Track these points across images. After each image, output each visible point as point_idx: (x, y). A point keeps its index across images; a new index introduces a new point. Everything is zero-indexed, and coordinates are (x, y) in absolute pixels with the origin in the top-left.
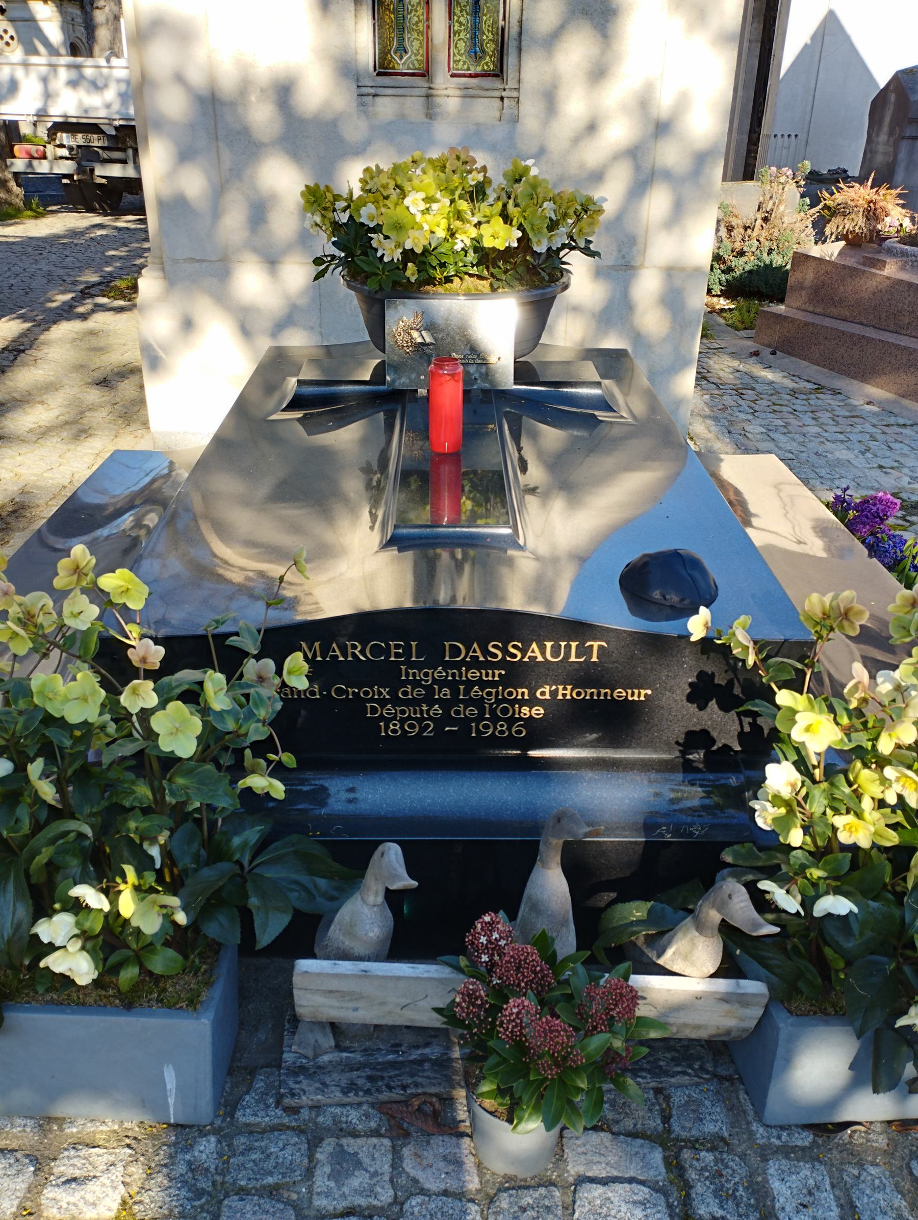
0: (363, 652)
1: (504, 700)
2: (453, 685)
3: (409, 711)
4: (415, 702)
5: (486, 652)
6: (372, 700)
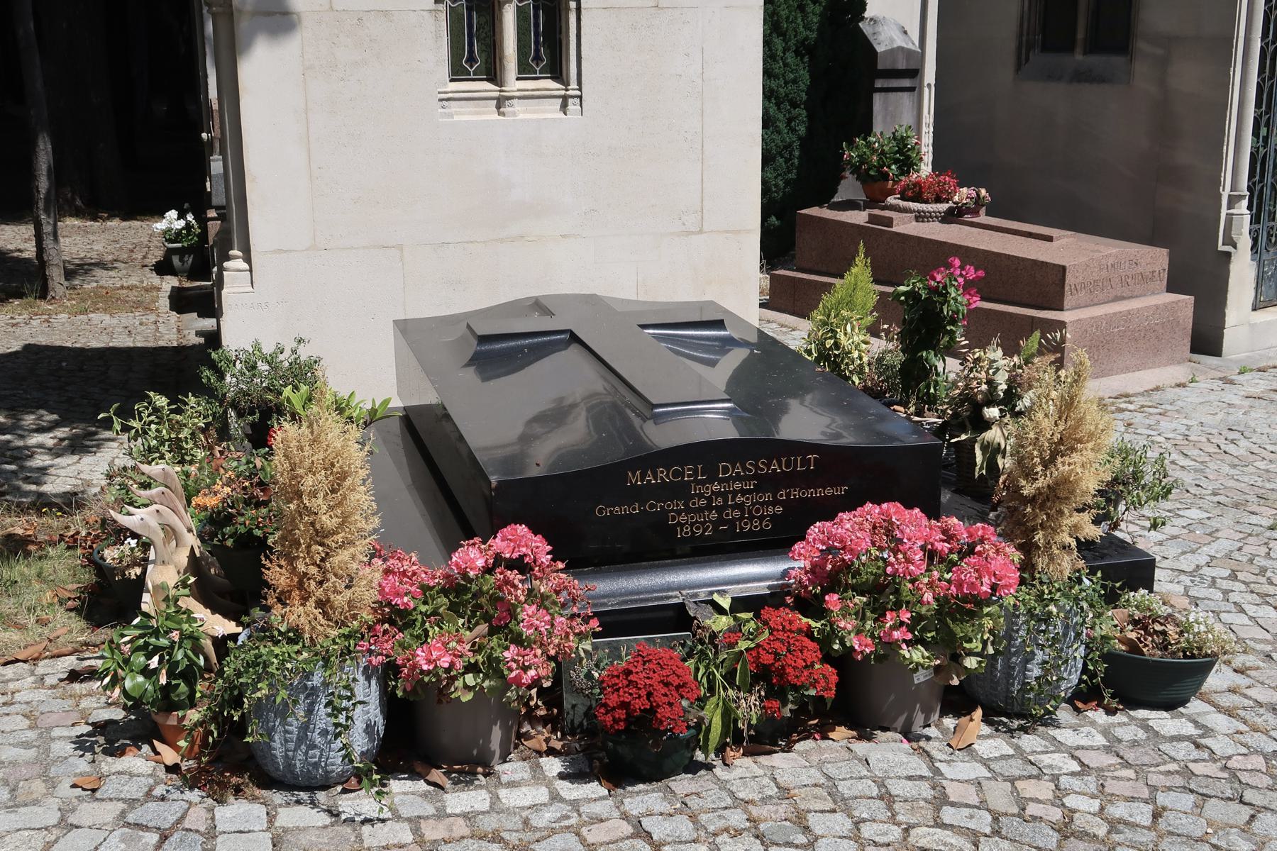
0: (667, 476)
1: (758, 503)
2: (724, 495)
3: (698, 518)
4: (701, 510)
5: (745, 469)
6: (673, 511)
